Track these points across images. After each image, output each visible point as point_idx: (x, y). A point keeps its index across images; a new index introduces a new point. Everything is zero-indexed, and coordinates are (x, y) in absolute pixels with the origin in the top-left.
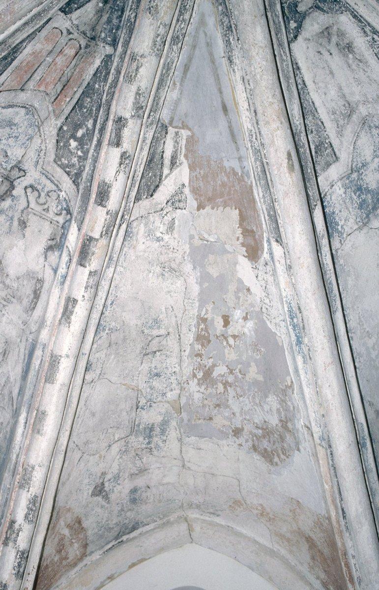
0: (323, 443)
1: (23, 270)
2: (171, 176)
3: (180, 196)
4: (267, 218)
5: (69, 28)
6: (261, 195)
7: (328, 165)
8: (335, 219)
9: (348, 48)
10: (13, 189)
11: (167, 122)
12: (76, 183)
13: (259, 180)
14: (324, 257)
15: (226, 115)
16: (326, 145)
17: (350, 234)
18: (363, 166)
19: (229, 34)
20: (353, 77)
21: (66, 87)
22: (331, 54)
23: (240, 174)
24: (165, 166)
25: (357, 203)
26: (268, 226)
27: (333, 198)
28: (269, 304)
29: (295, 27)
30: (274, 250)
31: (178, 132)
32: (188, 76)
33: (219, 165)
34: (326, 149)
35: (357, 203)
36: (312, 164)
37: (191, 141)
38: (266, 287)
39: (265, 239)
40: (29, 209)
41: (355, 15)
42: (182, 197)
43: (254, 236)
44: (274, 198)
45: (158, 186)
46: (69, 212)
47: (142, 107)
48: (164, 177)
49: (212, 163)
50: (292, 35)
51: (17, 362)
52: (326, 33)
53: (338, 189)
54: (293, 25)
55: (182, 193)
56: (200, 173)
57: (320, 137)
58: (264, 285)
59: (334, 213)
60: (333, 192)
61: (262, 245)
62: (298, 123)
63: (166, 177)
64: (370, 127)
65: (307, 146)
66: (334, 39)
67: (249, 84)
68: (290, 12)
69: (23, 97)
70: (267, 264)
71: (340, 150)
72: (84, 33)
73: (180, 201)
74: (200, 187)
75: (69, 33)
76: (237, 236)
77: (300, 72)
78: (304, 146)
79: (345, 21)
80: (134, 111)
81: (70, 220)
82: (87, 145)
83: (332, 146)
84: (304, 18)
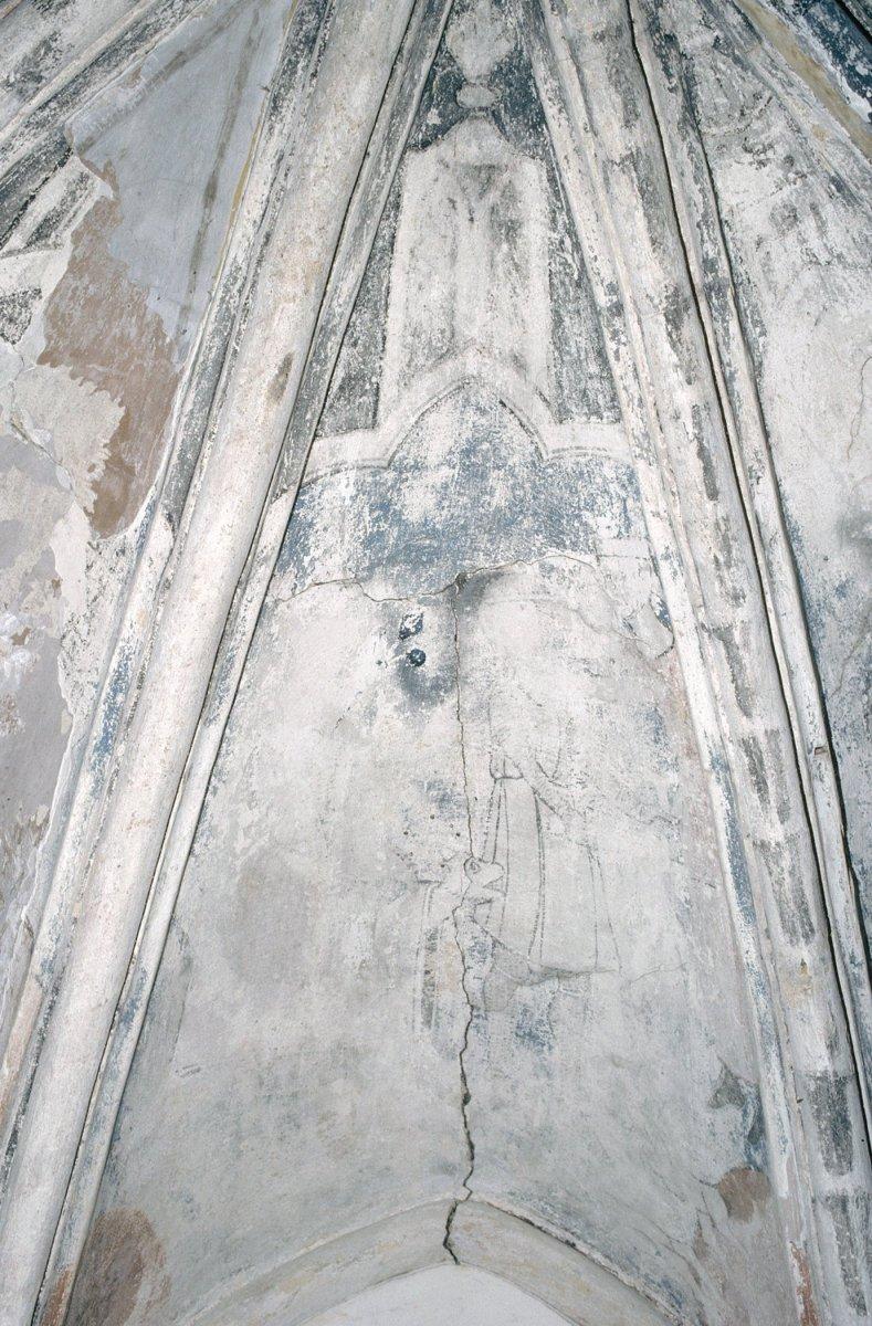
0: (46, 978)
2: (21, 256)
3: (17, 310)
4: (175, 460)
6: (189, 406)
7: (352, 426)
8: (307, 539)
9: (509, 229)
11: (75, 141)
13: (202, 375)
14: (244, 602)
15: (205, 207)
16: (368, 387)
17: (321, 583)
18: (416, 467)
19: (302, 51)
20: (488, 287)
22: (472, 220)
23: (168, 340)
24: (20, 228)
25: (366, 532)
26: (168, 479)
27: (326, 495)
28: (84, 637)
29: (435, 125)
30: (153, 534)
31: (88, 177)
32: (173, 79)
33: (136, 298)
34: (364, 393)
35: (366, 532)
36: (321, 406)
37: (104, 213)
38: (96, 598)
39: (148, 501)
41: (554, 177)
42: (20, 314)
43: (128, 482)
44: (210, 429)
47: (39, 79)
49: (125, 283)
50: (420, 136)
52: (486, 174)
53: (345, 482)
54: (433, 118)
55: (25, 305)
56: (86, 288)
57: (364, 363)
58: (95, 592)
59: (311, 525)
60: (331, 484)
61: (135, 509)
62: (338, 310)
63: (10, 253)
64: (467, 400)
65: (330, 366)
66: (493, 197)
67: (286, 175)
68: (441, 90)
70: (123, 552)
71: (388, 411)
73: (11, 320)
74: (71, 316)
76: (93, 461)
77: (396, 216)
78: (326, 363)
79: (531, 175)
80: (18, 76)
83: (377, 394)
84: (461, 119)
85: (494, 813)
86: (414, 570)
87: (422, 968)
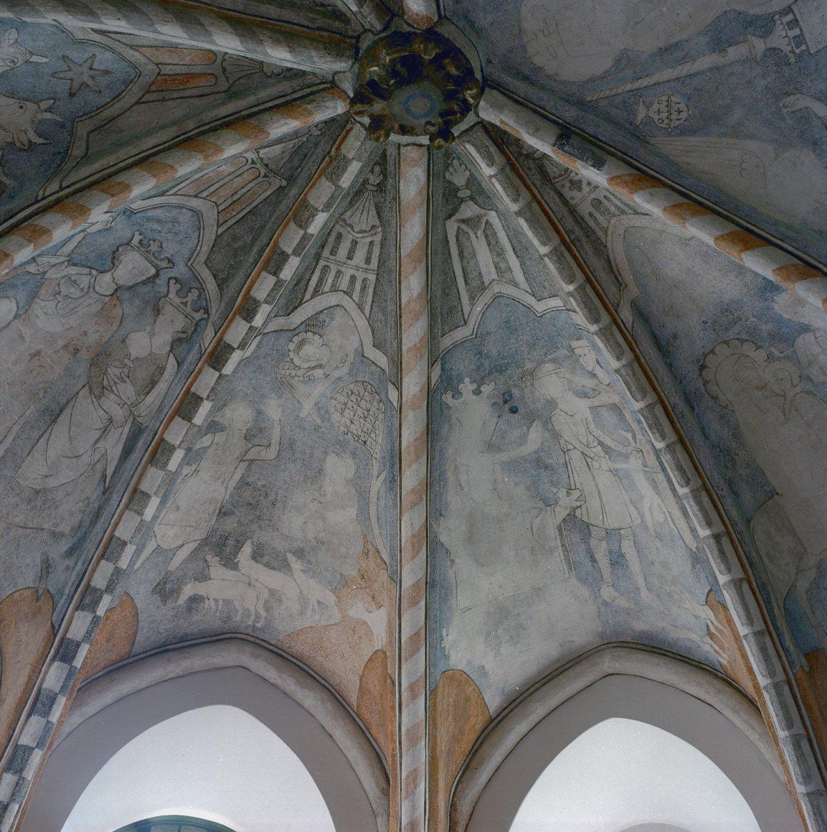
1: (144, 354)
5: (255, 159)
10: (158, 277)
12: (221, 286)
21: (236, 203)
22: (477, 237)
40: (167, 298)
45: (296, 308)
46: (207, 311)
48: (304, 301)
51: (118, 441)
58: (373, 420)
63: (305, 302)
69: (194, 203)
72: (267, 165)
75: (253, 162)
81: (207, 320)
82: (241, 256)
84: (461, 203)
85: (569, 467)
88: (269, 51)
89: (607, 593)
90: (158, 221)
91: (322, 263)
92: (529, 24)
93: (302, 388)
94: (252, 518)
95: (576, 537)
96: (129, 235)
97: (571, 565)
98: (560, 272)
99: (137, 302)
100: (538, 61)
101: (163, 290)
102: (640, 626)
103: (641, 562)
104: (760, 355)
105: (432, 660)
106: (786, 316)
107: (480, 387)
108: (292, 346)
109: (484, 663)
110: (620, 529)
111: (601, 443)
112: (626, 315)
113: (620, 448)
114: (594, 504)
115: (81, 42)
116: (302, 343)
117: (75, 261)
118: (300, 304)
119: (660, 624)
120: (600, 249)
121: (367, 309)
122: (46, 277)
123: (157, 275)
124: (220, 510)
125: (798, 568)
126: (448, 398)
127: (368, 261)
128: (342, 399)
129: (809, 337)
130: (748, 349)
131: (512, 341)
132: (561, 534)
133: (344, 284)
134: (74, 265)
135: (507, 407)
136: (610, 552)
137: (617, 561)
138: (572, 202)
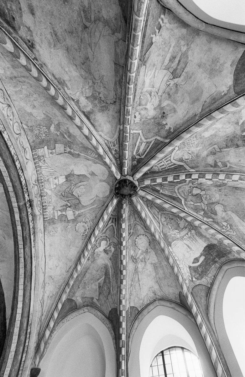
69: (176, 191)
75: (162, 189)
86: (159, 123)
87: (183, 73)
88: (140, 210)
89: (184, 49)
90: (184, 194)
91: (169, 168)
92: (106, 176)
93: (196, 152)
94: (235, 139)
95: (178, 71)
96: (190, 196)
97: (186, 64)
98: (126, 147)
99: (202, 187)
100: (108, 172)
101: (196, 185)
102: (184, 31)
103: (166, 57)
104: (101, 95)
105: (229, 99)
106: (90, 103)
107: (165, 125)
108: (188, 161)
109: (229, 66)
110: (164, 69)
111: (151, 96)
112: (121, 128)
113: (146, 93)
114: (166, 79)
115: (163, 225)
116: (187, 159)
117: (201, 201)
118: (179, 165)
119: (176, 31)
120: (119, 138)
121: (169, 156)
122: (207, 203)
123: (194, 187)
124: (237, 147)
125: (119, 41)
126: (172, 130)
127: (161, 162)
128: (191, 145)
129: (87, 95)
130: (103, 99)
131: (151, 128)
132: (181, 75)
133: (169, 162)
134: (202, 200)
135: (164, 115)
136: (173, 62)
137: (173, 58)
138: (119, 148)
